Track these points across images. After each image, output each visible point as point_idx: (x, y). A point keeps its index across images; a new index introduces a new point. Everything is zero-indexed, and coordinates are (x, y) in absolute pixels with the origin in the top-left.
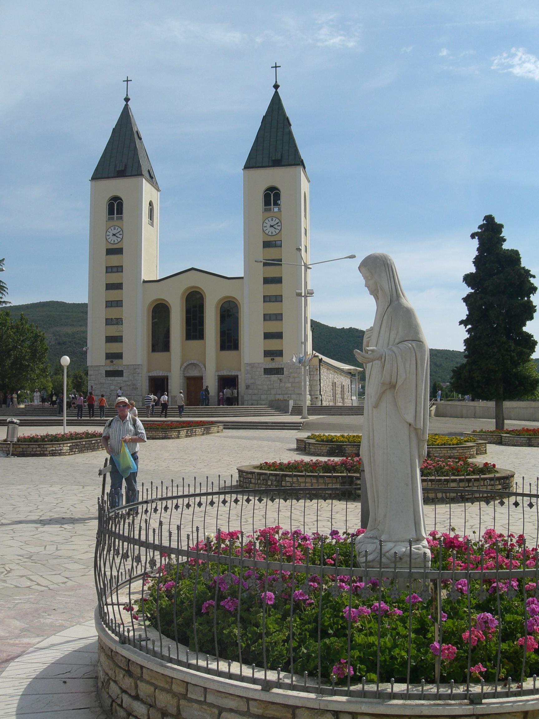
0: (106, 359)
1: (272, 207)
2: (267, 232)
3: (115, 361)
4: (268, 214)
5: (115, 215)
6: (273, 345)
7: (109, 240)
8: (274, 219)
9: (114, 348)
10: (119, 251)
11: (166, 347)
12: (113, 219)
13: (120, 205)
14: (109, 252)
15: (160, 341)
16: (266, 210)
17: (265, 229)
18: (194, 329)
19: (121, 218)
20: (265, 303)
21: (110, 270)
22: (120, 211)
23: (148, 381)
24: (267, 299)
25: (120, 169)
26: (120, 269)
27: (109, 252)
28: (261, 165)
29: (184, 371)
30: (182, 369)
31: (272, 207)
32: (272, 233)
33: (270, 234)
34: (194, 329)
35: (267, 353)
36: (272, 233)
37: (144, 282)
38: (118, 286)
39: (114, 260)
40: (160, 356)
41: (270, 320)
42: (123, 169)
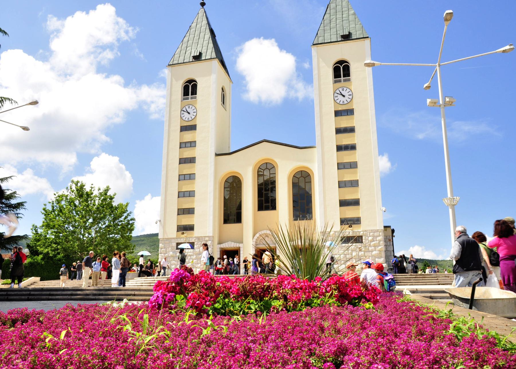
0: (178, 231)
1: (342, 78)
2: (338, 101)
3: (187, 234)
4: (338, 85)
5: (190, 96)
6: (350, 212)
7: (184, 118)
8: (345, 89)
9: (186, 220)
10: (193, 128)
11: (238, 219)
12: (188, 99)
13: (195, 87)
14: (184, 129)
15: (232, 214)
16: (335, 82)
17: (336, 99)
18: (266, 200)
19: (195, 98)
20: (339, 170)
21: (184, 145)
22: (194, 92)
23: (219, 253)
24: (341, 166)
25: (195, 55)
26: (193, 144)
27: (184, 129)
28: (329, 41)
29: (256, 242)
30: (255, 240)
31: (342, 78)
32: (343, 102)
33: (341, 103)
34: (266, 200)
35: (343, 221)
36: (343, 102)
37: (217, 155)
38: (192, 160)
39: (188, 136)
40: (232, 227)
41: (345, 187)
42: (198, 54)
